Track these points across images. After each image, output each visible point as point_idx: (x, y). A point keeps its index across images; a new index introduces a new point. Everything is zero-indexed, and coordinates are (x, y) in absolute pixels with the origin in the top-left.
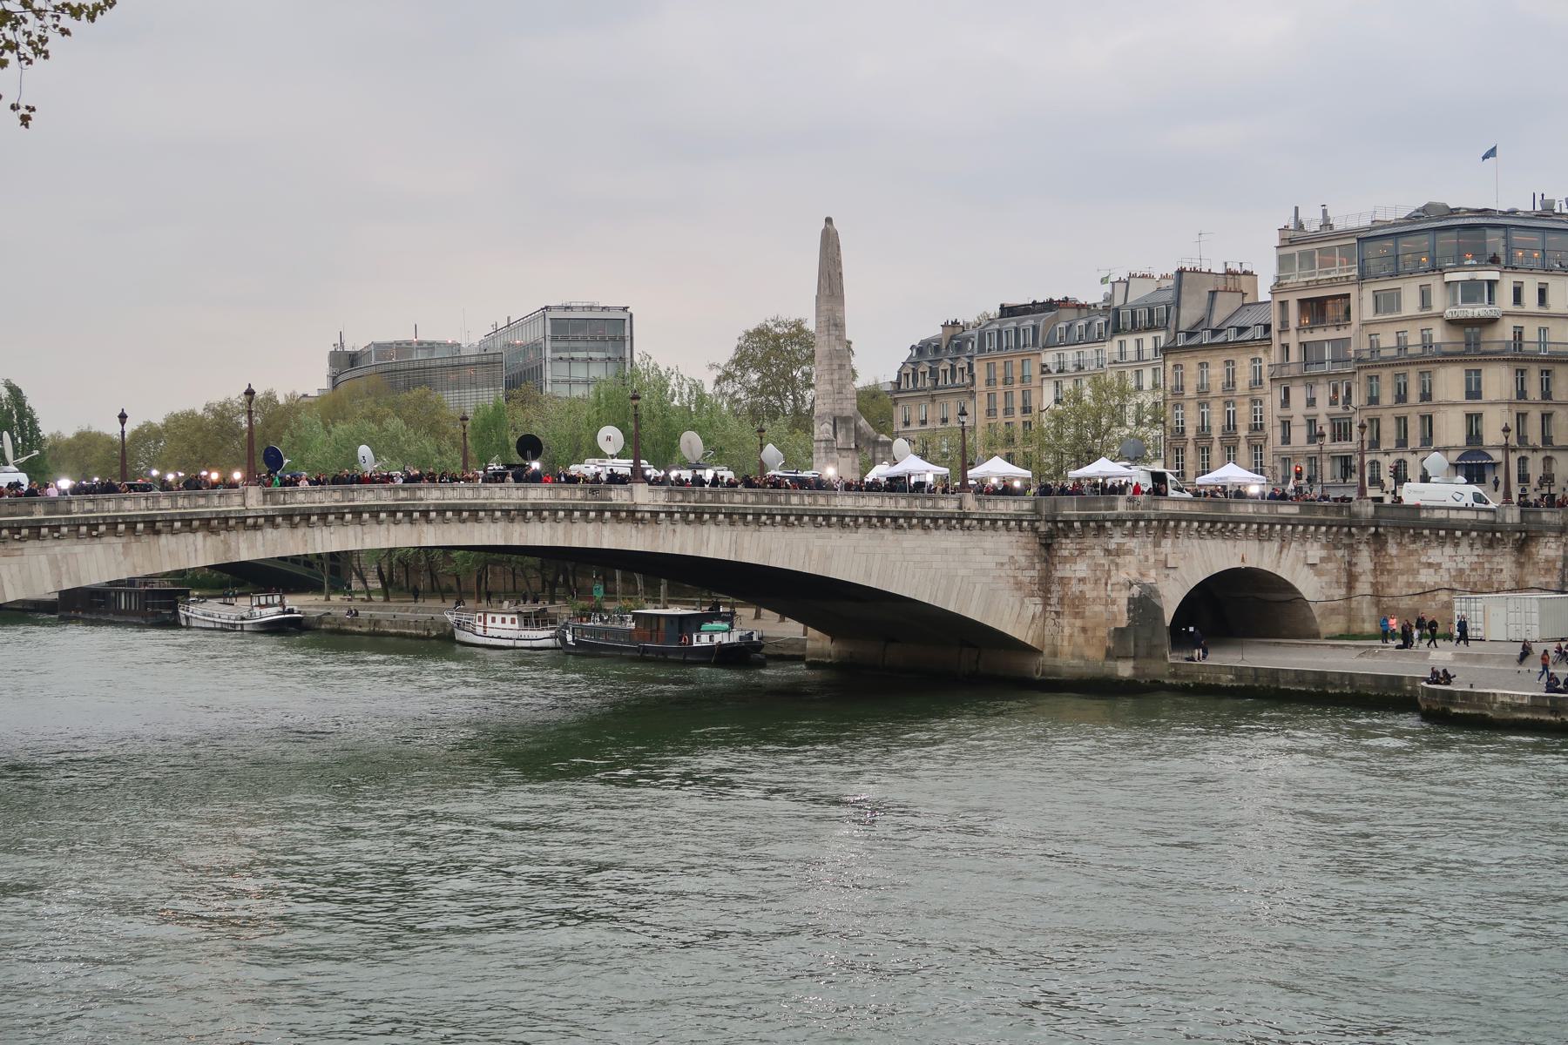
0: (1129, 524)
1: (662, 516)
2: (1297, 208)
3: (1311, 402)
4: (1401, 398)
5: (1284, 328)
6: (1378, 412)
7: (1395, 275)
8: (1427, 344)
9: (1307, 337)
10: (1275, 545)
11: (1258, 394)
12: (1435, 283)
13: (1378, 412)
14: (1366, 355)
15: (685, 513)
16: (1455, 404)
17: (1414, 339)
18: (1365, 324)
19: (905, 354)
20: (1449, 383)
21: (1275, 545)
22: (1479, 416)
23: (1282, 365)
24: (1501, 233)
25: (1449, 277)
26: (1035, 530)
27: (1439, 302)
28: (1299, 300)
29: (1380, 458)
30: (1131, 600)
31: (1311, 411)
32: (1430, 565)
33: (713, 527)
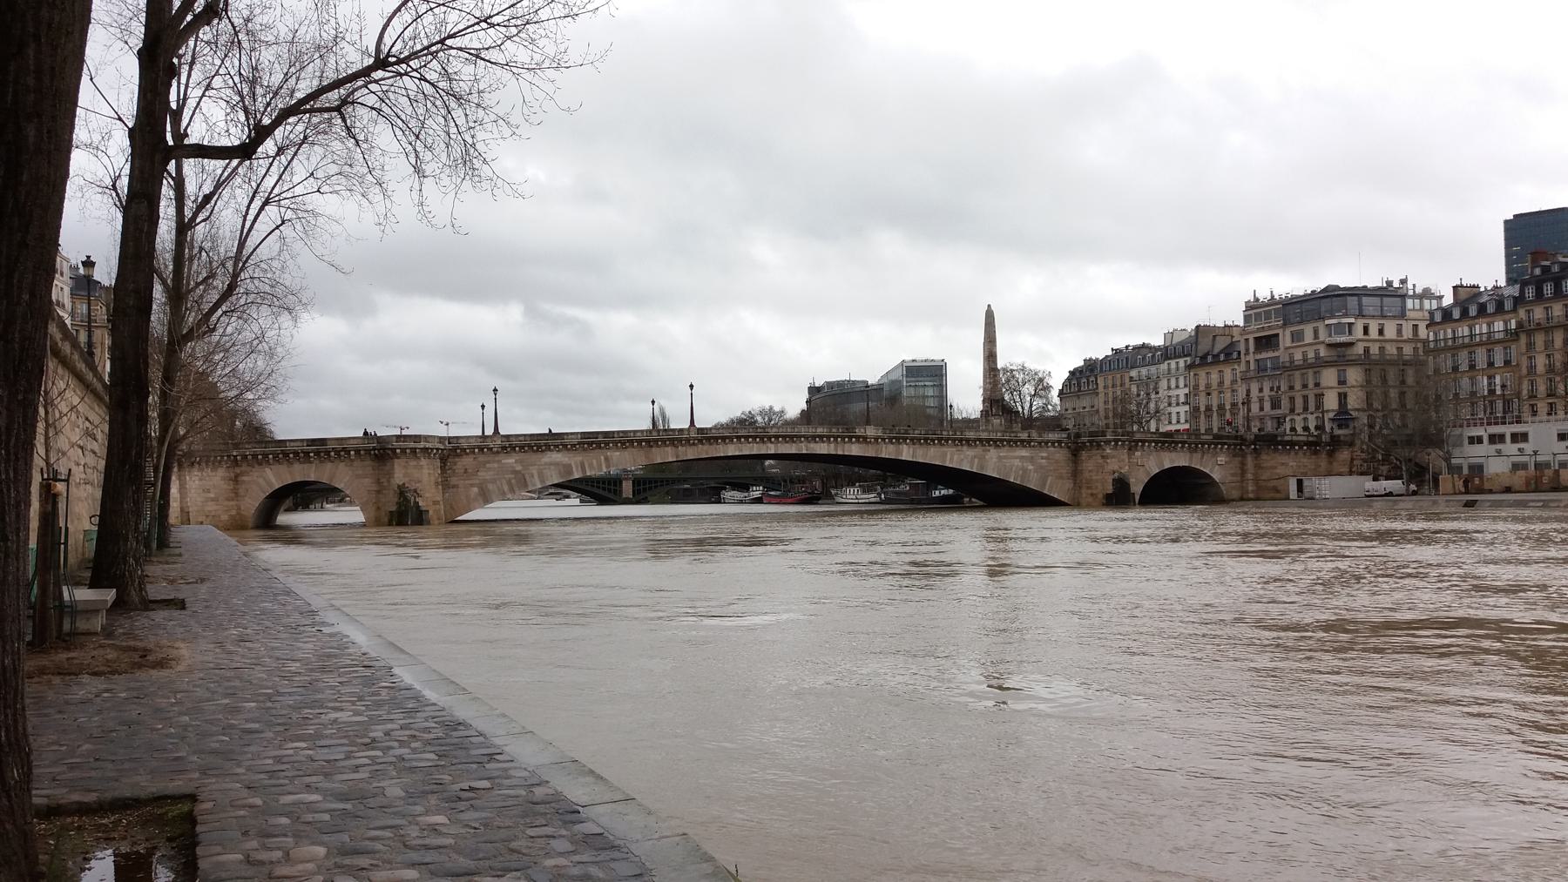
0: (1113, 443)
1: (880, 440)
2: (1255, 291)
3: (1261, 390)
4: (1305, 386)
5: (1247, 353)
6: (1294, 393)
7: (1301, 322)
8: (1317, 357)
9: (1259, 357)
10: (1199, 455)
11: (1235, 387)
12: (1321, 326)
13: (1307, 392)
14: (1288, 364)
15: (891, 439)
16: (1331, 388)
17: (1311, 355)
18: (1287, 348)
19: (1067, 375)
20: (1329, 377)
21: (1199, 455)
22: (1345, 395)
23: (1247, 372)
24: (1356, 298)
25: (1327, 322)
26: (1069, 447)
27: (1323, 336)
28: (1255, 338)
29: (1296, 418)
30: (1113, 480)
31: (1261, 395)
33: (905, 446)
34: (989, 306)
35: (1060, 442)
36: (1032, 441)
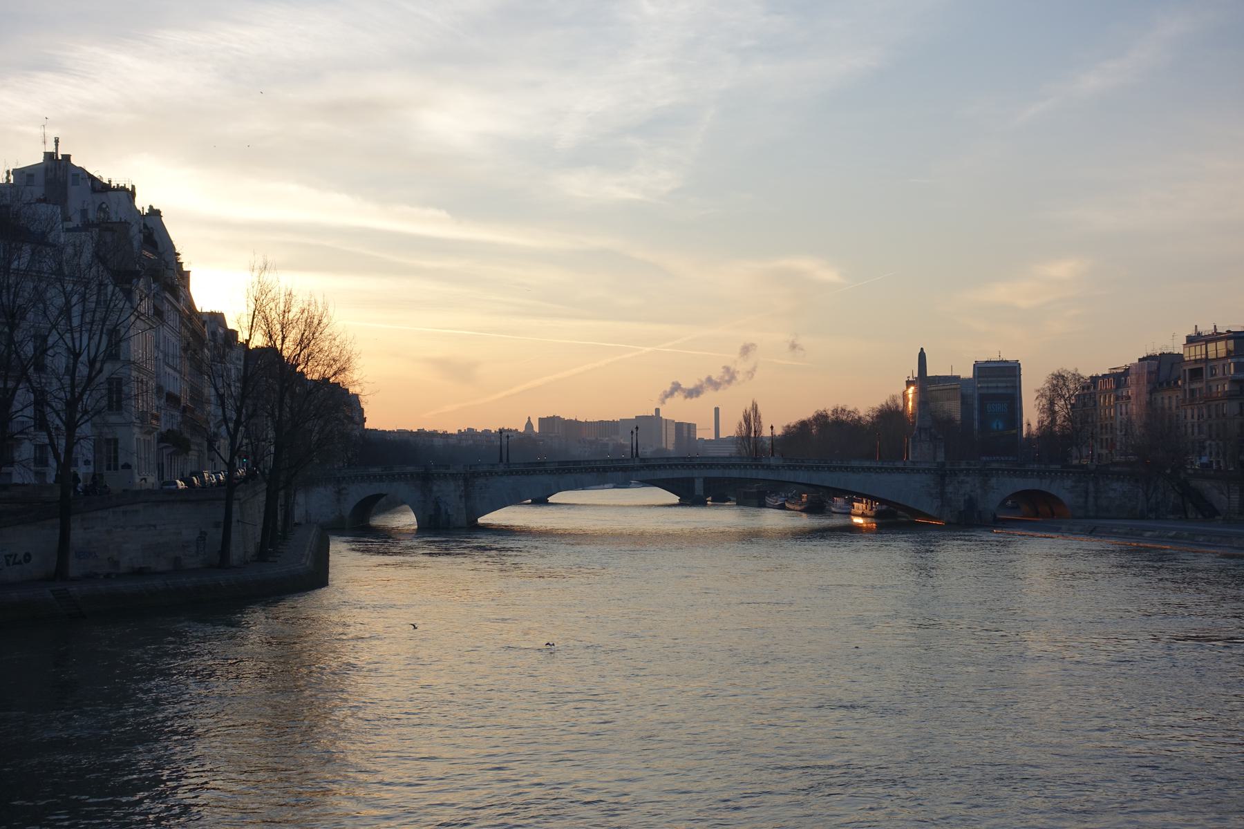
0: (965, 472)
9: (1193, 386)
15: (789, 466)
30: (965, 500)
32: (1113, 489)
34: (922, 349)
35: (929, 470)
36: (906, 469)
